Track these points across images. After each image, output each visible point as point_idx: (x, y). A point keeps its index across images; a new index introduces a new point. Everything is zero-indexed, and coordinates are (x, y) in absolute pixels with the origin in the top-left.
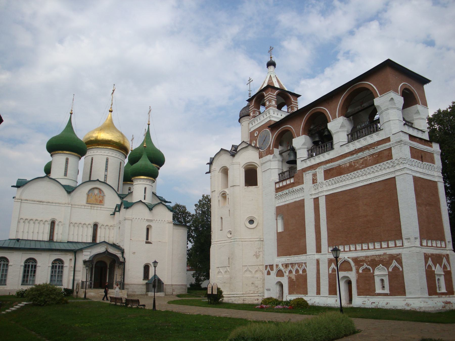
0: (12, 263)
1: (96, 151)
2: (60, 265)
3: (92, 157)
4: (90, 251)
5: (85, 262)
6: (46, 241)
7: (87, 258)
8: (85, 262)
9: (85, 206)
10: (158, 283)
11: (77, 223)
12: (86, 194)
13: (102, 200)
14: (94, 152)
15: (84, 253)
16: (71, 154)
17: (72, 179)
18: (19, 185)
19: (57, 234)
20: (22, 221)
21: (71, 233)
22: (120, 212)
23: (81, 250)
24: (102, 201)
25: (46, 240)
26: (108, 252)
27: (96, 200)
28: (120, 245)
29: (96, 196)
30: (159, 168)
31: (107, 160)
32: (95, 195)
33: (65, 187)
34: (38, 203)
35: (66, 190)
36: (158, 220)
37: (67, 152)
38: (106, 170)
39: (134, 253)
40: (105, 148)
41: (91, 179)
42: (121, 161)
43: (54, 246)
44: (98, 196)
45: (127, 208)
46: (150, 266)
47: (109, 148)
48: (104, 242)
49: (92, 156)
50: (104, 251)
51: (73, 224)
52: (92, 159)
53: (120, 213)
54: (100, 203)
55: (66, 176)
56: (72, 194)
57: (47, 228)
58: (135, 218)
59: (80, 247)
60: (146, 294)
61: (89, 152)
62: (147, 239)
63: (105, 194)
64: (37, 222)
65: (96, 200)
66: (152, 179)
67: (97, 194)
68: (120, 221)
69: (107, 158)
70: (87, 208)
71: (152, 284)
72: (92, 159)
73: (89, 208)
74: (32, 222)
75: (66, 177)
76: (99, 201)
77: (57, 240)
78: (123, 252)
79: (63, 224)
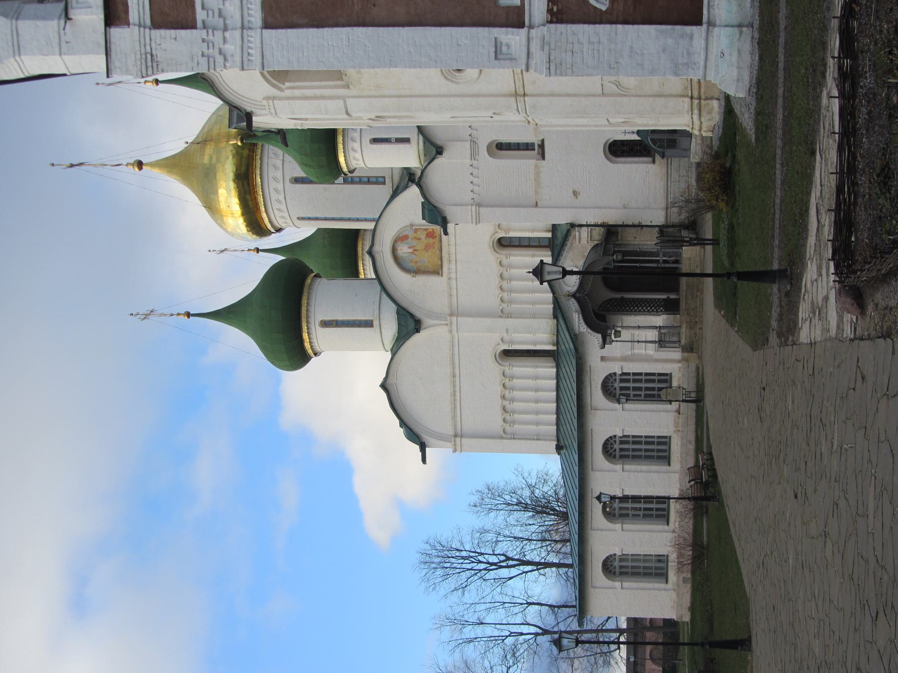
0: (618, 489)
2: (618, 380)
3: (299, 218)
9: (450, 279)
12: (414, 279)
13: (425, 233)
16: (308, 317)
19: (535, 344)
26: (578, 291)
27: (427, 247)
32: (415, 252)
33: (402, 338)
37: (305, 336)
39: (575, 194)
44: (415, 244)
47: (261, 181)
49: (295, 220)
50: (576, 304)
54: (436, 237)
55: (372, 321)
56: (418, 314)
57: (522, 369)
65: (427, 247)
66: (340, 139)
67: (409, 248)
70: (455, 271)
73: (453, 266)
75: (376, 323)
76: (431, 240)
77: (554, 345)
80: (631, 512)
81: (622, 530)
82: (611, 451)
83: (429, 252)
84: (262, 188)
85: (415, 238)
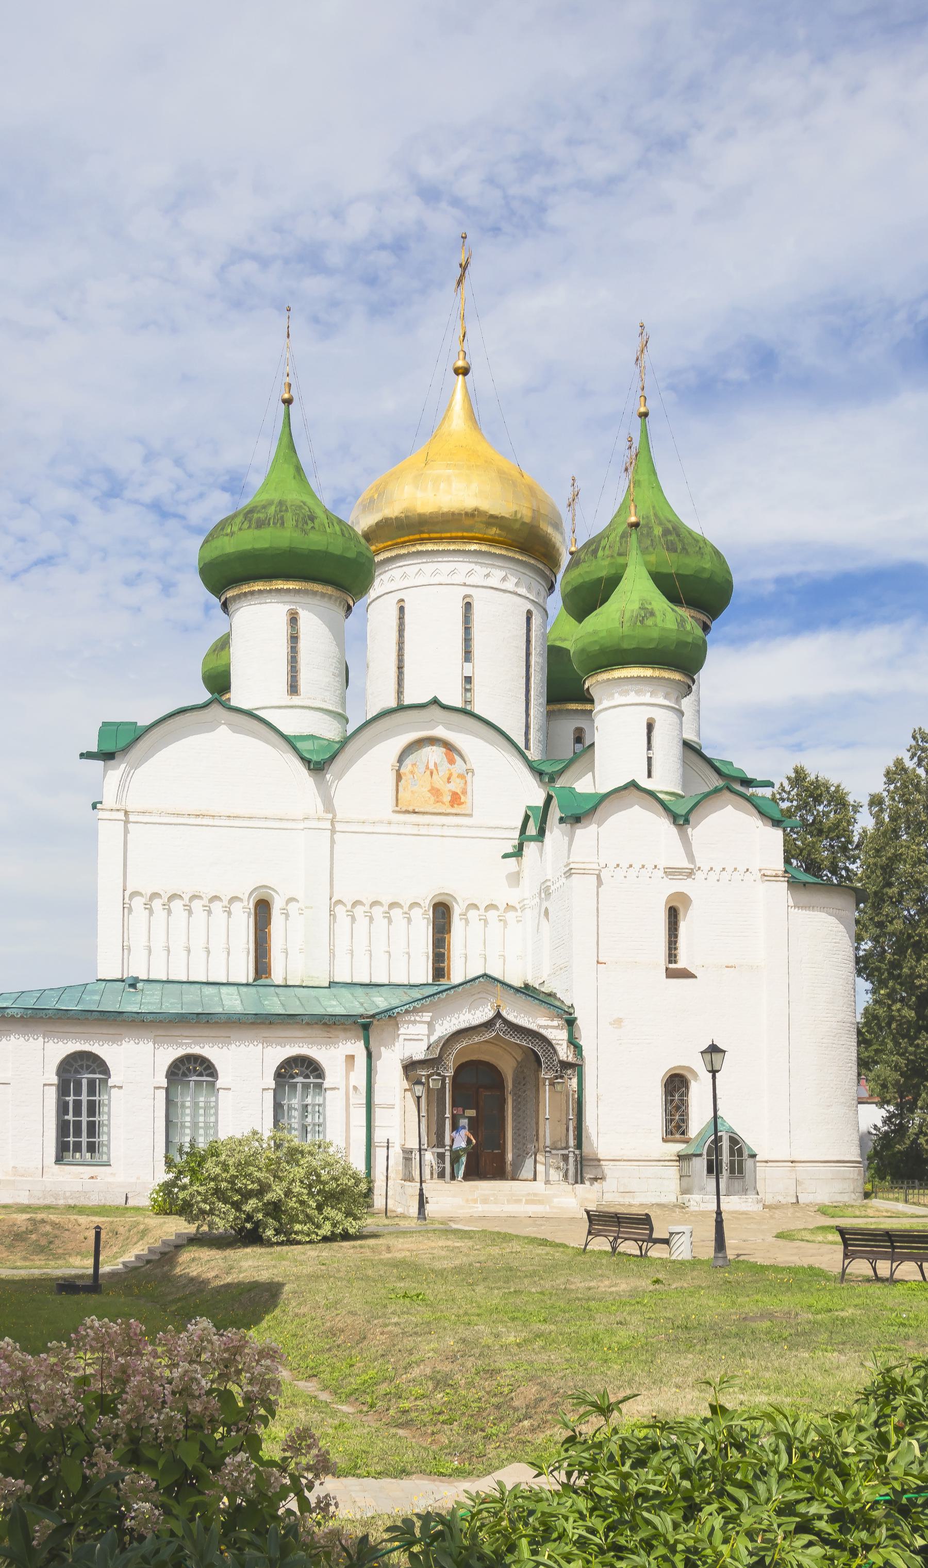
1: (415, 568)
4: (428, 1019)
5: (410, 1067)
6: (242, 985)
7: (419, 1052)
8: (410, 1067)
10: (732, 1153)
11: (364, 901)
14: (405, 576)
15: (405, 1030)
17: (321, 706)
18: (109, 748)
20: (138, 903)
21: (342, 944)
22: (542, 842)
23: (390, 1017)
24: (462, 797)
25: (244, 981)
26: (506, 1022)
27: (436, 792)
28: (554, 991)
29: (432, 773)
30: (708, 622)
31: (468, 606)
32: (428, 772)
34: (193, 821)
35: (303, 759)
36: (718, 869)
38: (468, 655)
39: (618, 1022)
40: (454, 551)
41: (407, 701)
42: (530, 606)
43: (274, 1004)
44: (441, 774)
45: (575, 819)
46: (689, 1076)
47: (469, 551)
48: (485, 975)
51: (344, 905)
52: (402, 609)
53: (541, 851)
58: (612, 865)
59: (380, 1002)
60: (680, 1201)
61: (385, 577)
62: (672, 956)
63: (474, 767)
64: (197, 905)
65: (436, 792)
66: (677, 676)
67: (435, 764)
68: (548, 884)
69: (465, 597)
71: (705, 1156)
72: (402, 609)
74: (177, 905)
75: (296, 701)
76: (447, 798)
78: (571, 1023)
79: (306, 908)
80: (71, 1099)
81: (45, 1085)
82: (76, 1065)
83: (429, 795)
84: (459, 551)
85: (451, 775)
